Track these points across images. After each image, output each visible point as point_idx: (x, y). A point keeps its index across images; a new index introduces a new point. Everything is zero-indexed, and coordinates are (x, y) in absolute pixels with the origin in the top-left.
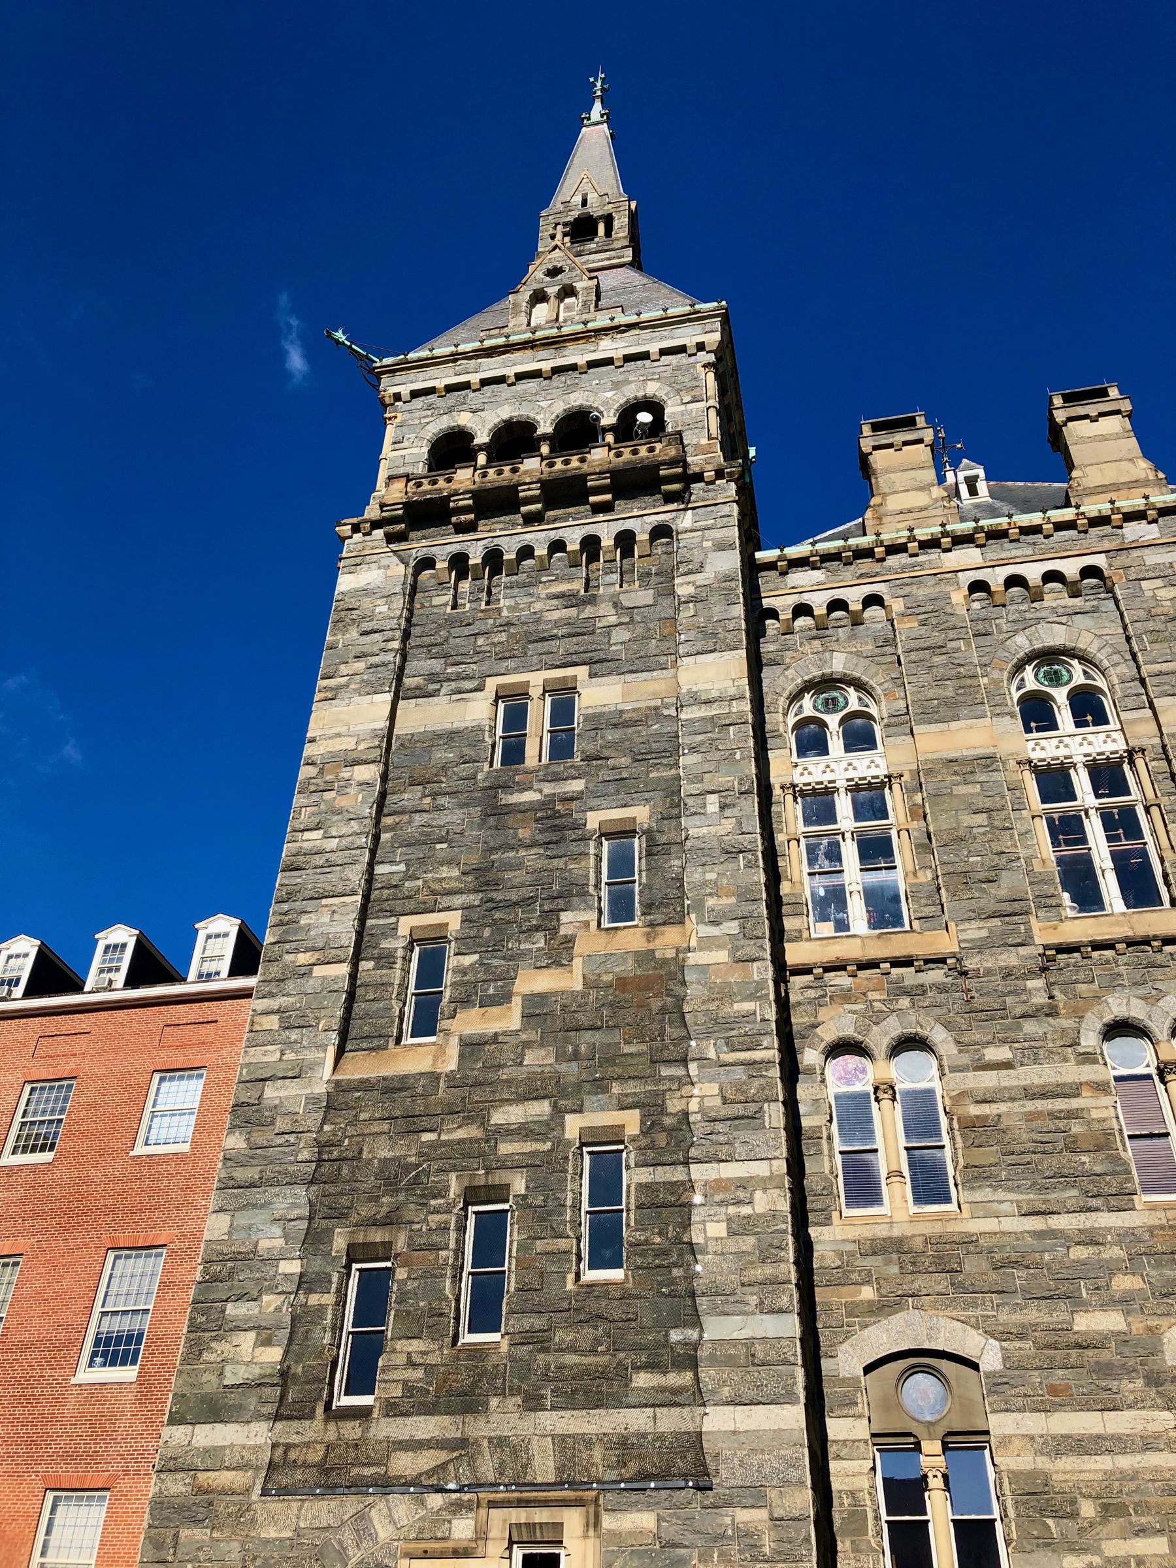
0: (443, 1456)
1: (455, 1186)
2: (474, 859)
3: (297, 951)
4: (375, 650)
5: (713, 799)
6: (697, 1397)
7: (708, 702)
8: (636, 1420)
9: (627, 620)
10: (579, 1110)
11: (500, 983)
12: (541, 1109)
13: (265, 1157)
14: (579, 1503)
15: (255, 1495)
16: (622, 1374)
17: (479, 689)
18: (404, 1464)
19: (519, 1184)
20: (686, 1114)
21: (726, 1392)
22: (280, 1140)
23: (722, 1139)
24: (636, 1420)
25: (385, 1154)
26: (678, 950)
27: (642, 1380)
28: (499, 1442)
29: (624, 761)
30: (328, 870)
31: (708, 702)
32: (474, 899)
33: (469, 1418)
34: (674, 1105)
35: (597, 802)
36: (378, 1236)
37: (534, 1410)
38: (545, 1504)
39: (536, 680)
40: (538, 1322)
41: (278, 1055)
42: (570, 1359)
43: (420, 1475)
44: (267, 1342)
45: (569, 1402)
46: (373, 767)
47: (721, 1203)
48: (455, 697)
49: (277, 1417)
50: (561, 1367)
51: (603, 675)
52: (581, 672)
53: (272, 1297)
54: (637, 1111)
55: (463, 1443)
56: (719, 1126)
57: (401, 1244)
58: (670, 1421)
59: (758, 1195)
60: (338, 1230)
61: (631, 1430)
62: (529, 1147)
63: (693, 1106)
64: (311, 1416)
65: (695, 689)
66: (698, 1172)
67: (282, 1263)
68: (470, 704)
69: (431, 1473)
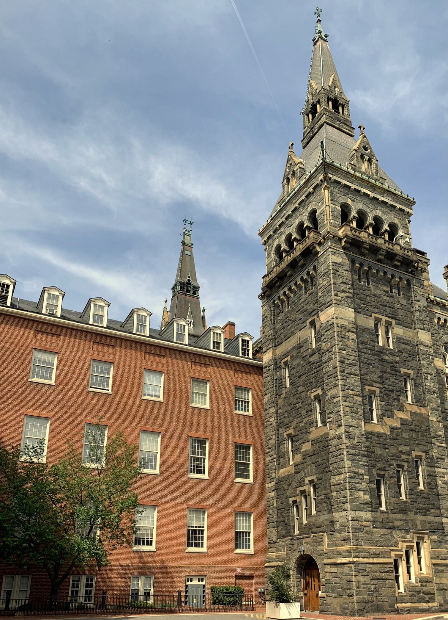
0: (403, 522)
1: (395, 463)
2: (380, 374)
3: (348, 389)
4: (347, 291)
5: (429, 376)
6: (440, 515)
7: (425, 346)
8: (432, 519)
9: (402, 308)
10: (414, 451)
11: (390, 412)
12: (408, 448)
13: (355, 448)
14: (427, 534)
15: (371, 527)
16: (428, 510)
17: (371, 316)
18: (397, 524)
19: (406, 466)
20: (433, 456)
21: (445, 515)
22: (358, 444)
23: (439, 463)
24: (432, 519)
25: (380, 453)
26: (427, 415)
27: (432, 511)
28: (412, 520)
29: (406, 355)
30: (350, 366)
31: (425, 346)
32: (381, 386)
33: (406, 515)
34: (431, 453)
35: (403, 366)
36: (382, 473)
37: (416, 515)
38: (422, 533)
39: (384, 318)
40: (414, 497)
41: (351, 420)
42: (422, 506)
43: (399, 526)
44: (365, 494)
45: (421, 513)
46: (354, 334)
47: (440, 477)
48: (365, 316)
49: (372, 511)
50: (420, 507)
51: (398, 325)
52: (394, 322)
53: (364, 484)
54: (424, 453)
55: (405, 520)
56: (439, 460)
57: (387, 475)
58: (437, 519)
59: (445, 476)
60: (374, 470)
61: (432, 520)
62: (407, 457)
63: (434, 455)
64: (377, 512)
65: (422, 340)
66: (437, 470)
67: (364, 476)
68: (369, 320)
69: (401, 525)
